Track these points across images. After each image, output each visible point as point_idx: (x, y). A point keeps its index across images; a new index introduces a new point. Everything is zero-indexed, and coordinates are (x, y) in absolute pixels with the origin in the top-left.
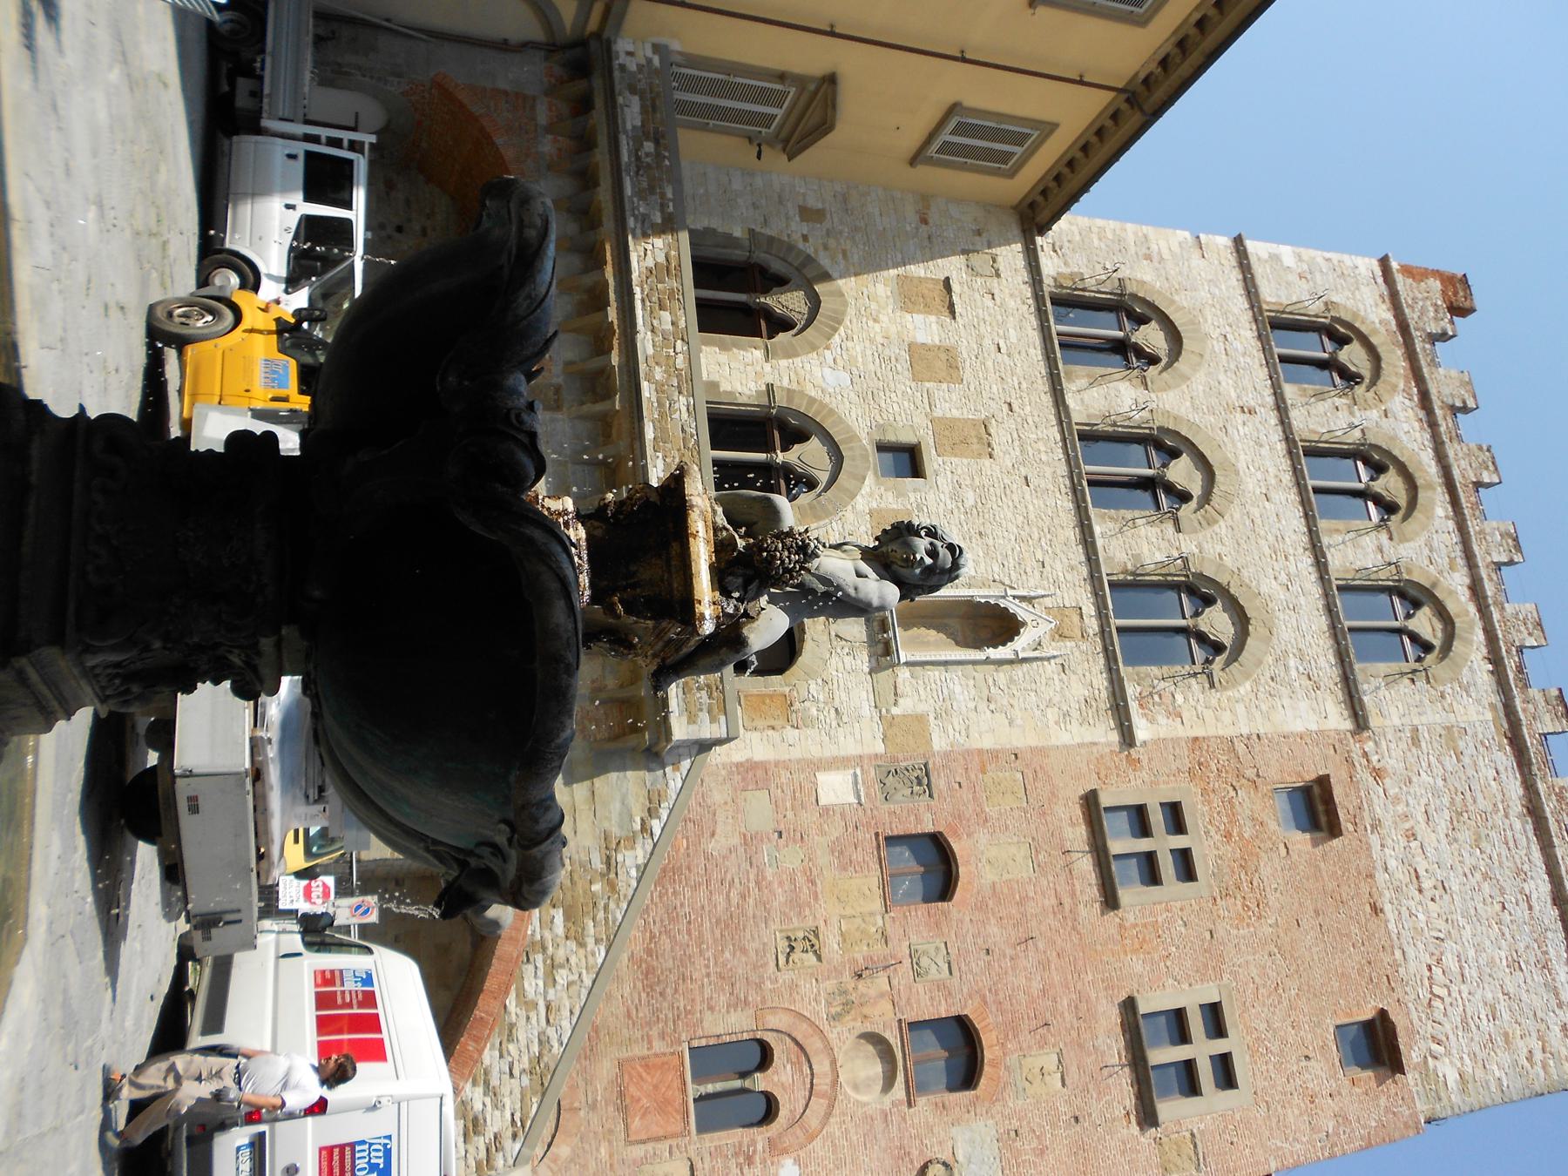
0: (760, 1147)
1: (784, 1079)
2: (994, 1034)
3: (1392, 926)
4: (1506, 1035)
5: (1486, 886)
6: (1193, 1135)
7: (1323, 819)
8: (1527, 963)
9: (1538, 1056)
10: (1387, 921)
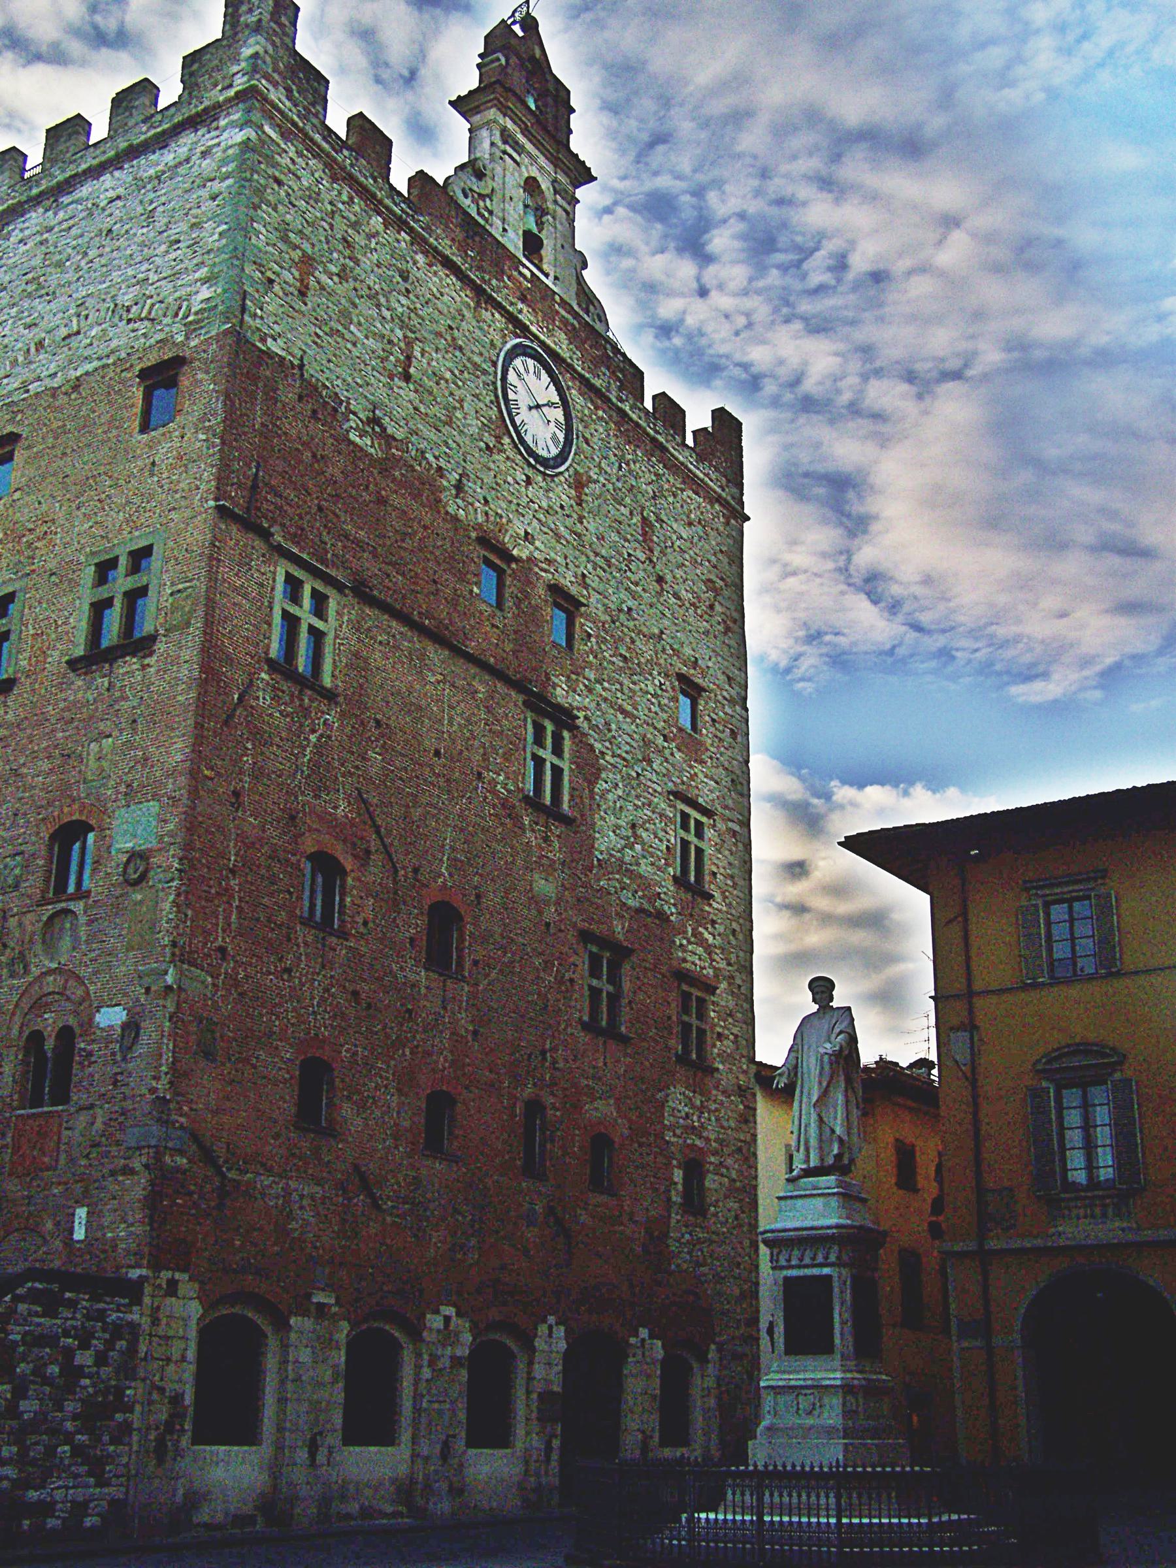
0: (82, 1045)
1: (51, 1021)
2: (66, 810)
3: (89, 367)
4: (193, 226)
5: (92, 253)
6: (172, 594)
7: (8, 449)
8: (152, 202)
9: (216, 186)
10: (87, 374)
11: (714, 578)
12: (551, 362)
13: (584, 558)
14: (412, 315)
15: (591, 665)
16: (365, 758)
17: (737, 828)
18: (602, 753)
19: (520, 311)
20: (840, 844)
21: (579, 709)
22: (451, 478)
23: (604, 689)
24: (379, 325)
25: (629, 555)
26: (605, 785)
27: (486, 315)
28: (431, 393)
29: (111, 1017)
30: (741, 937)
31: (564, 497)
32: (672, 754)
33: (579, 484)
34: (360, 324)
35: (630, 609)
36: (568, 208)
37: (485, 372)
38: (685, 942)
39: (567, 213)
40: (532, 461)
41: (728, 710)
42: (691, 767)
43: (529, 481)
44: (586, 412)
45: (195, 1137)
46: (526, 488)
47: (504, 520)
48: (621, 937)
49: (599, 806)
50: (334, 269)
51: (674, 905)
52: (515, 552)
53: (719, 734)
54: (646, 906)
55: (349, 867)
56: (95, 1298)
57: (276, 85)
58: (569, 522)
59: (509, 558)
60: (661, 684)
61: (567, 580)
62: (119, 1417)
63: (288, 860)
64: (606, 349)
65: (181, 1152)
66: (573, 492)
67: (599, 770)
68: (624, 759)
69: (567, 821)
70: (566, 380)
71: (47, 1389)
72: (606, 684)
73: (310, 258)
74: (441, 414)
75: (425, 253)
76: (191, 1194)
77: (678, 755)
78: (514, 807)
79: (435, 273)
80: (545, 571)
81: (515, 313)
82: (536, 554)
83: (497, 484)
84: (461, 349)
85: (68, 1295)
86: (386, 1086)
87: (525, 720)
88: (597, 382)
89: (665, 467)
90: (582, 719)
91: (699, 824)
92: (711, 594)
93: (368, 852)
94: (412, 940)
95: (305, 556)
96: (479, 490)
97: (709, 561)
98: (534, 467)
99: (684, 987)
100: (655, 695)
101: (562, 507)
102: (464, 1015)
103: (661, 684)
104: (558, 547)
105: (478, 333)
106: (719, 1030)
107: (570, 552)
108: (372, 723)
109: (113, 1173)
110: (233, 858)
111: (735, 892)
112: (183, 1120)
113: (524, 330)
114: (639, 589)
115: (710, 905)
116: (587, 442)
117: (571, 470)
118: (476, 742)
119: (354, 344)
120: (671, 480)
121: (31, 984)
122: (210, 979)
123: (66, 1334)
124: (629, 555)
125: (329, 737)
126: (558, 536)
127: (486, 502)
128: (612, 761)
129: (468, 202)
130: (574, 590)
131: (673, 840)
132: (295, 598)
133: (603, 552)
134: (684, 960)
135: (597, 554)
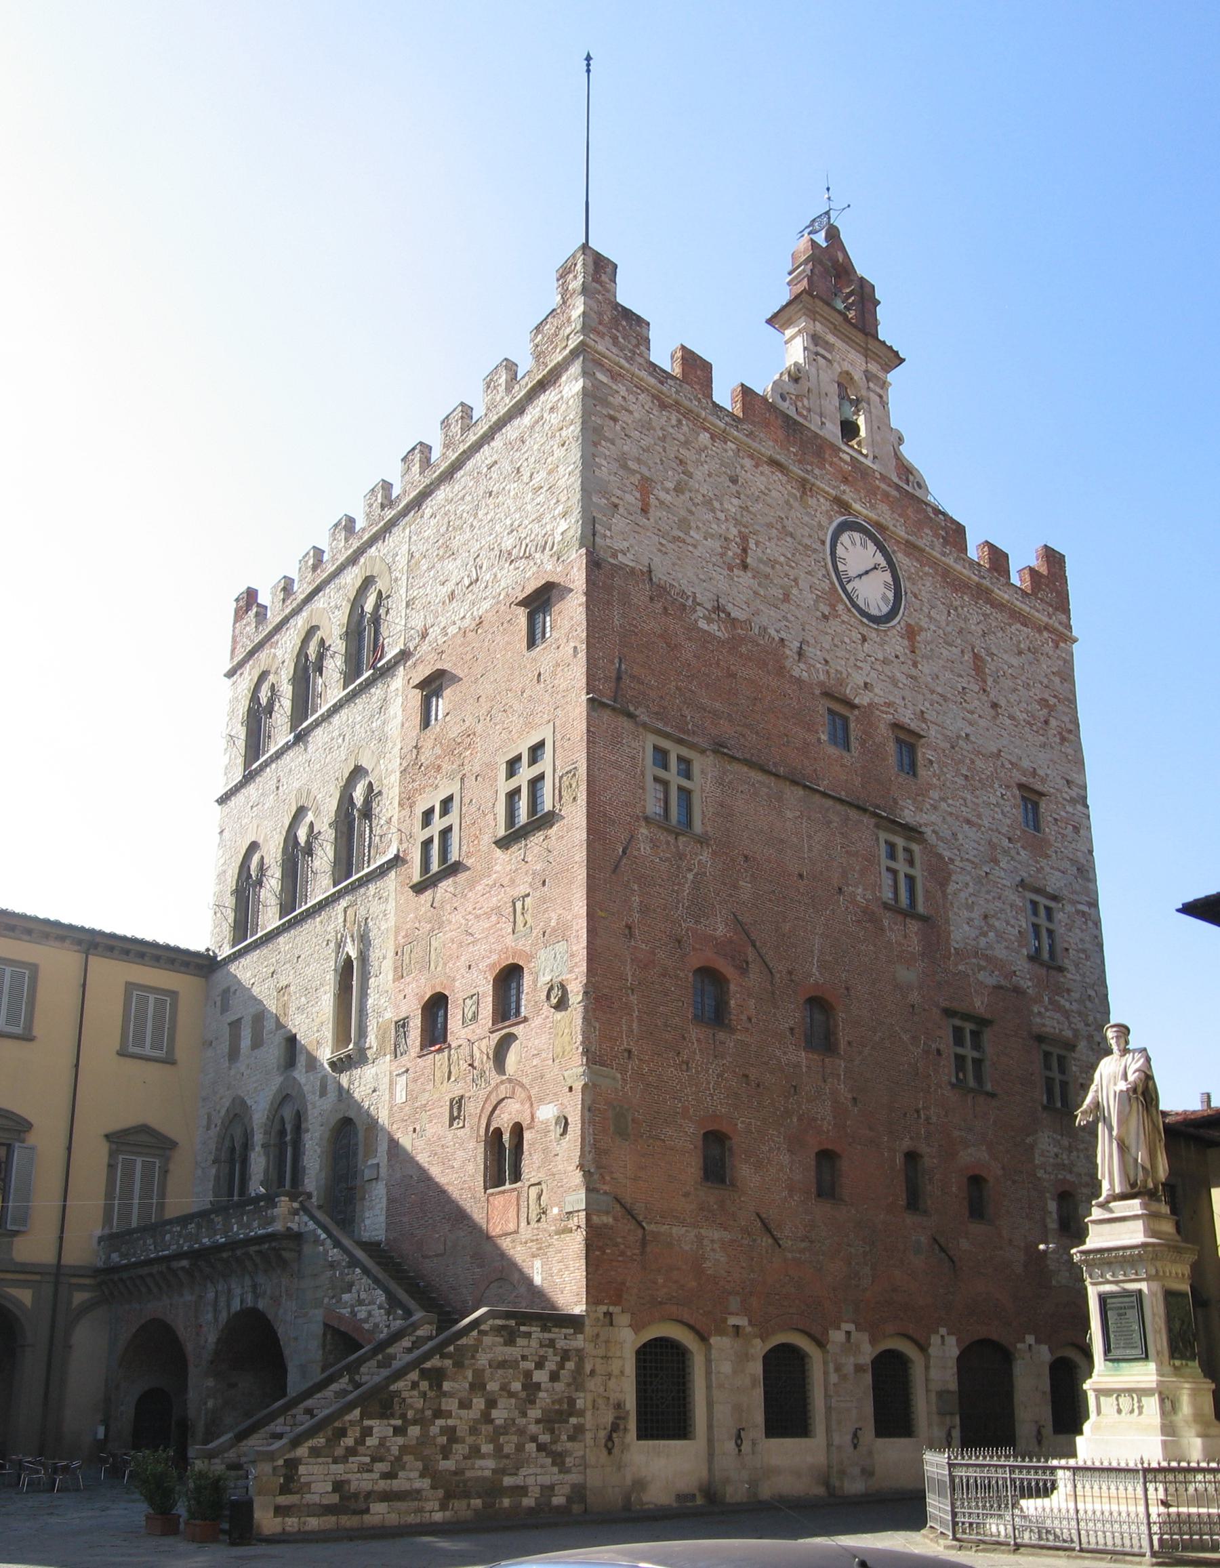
12: (876, 535)
13: (921, 697)
16: (735, 887)
20: (1178, 910)
21: (926, 825)
29: (547, 1113)
31: (898, 647)
33: (911, 633)
40: (865, 620)
43: (864, 639)
45: (618, 1200)
47: (844, 675)
52: (856, 701)
55: (729, 977)
56: (545, 1329)
58: (905, 668)
59: (853, 706)
61: (907, 717)
62: (573, 1420)
63: (677, 976)
64: (925, 511)
65: (607, 1213)
66: (906, 642)
69: (924, 919)
71: (513, 1401)
76: (616, 1245)
78: (873, 913)
83: (836, 646)
85: (522, 1328)
87: (877, 839)
88: (920, 543)
90: (929, 833)
93: (747, 963)
94: (792, 1029)
96: (819, 653)
101: (897, 657)
107: (907, 693)
108: (741, 859)
109: (558, 1233)
112: (606, 1188)
116: (916, 596)
117: (902, 623)
118: (835, 864)
121: (491, 1093)
122: (619, 1076)
123: (524, 1358)
127: (827, 662)
130: (913, 726)
132: (665, 767)
135: (933, 692)
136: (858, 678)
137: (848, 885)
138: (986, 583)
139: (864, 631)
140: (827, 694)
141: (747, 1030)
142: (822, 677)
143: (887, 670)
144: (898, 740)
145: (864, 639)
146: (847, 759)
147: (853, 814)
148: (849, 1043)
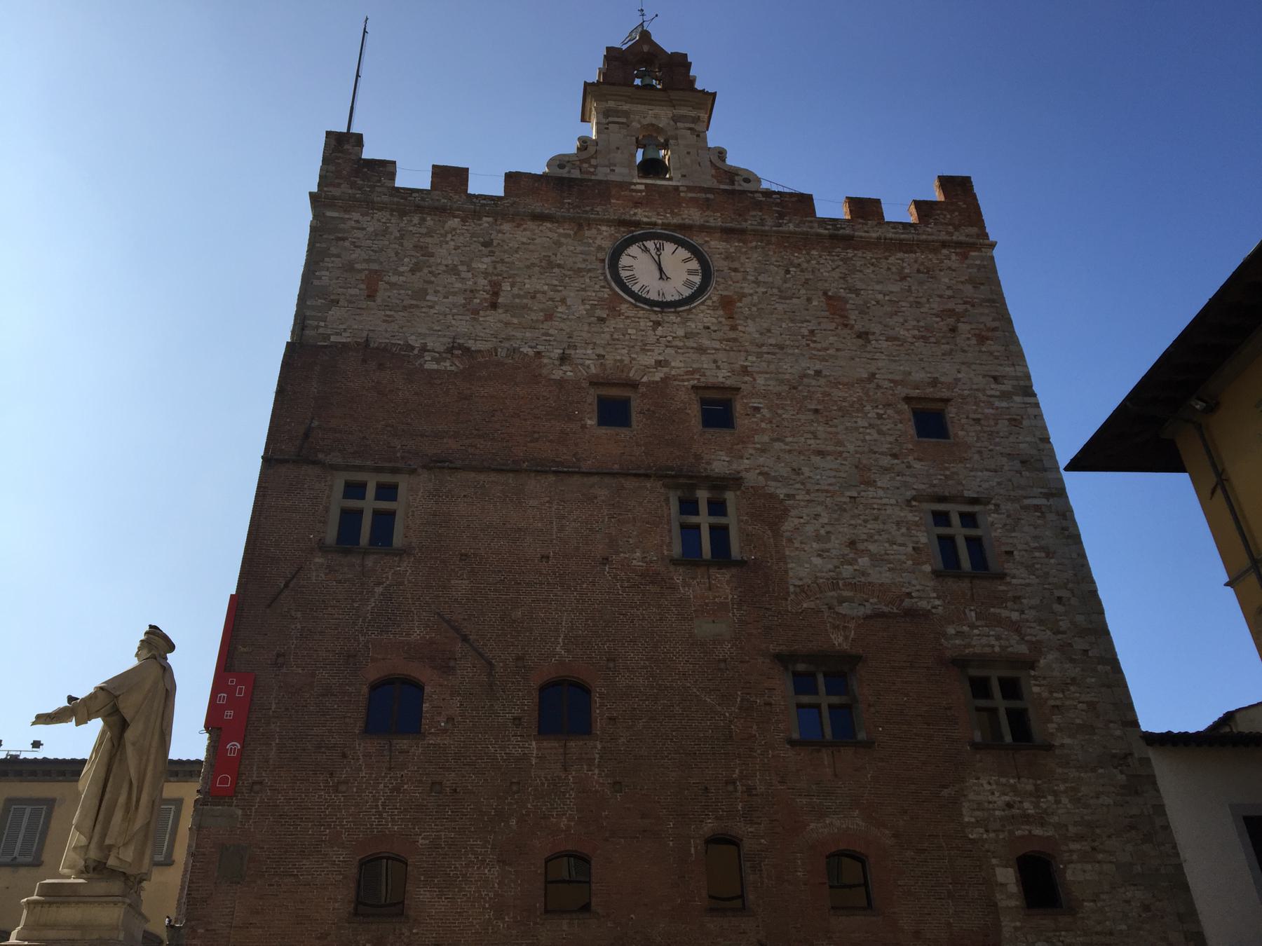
11: (950, 305)
12: (680, 235)
14: (499, 266)
15: (764, 431)
17: (1042, 501)
18: (790, 496)
19: (635, 214)
21: (747, 470)
22: (552, 355)
23: (786, 444)
24: (458, 285)
25: (812, 332)
26: (796, 521)
27: (594, 231)
28: (525, 307)
30: (1074, 601)
32: (909, 467)
33: (727, 304)
34: (436, 292)
35: (818, 373)
36: (692, 126)
37: (589, 271)
38: (965, 628)
39: (690, 129)
41: (1004, 404)
42: (947, 469)
44: (732, 250)
46: (654, 330)
48: (845, 646)
49: (790, 540)
50: (401, 269)
51: (938, 598)
53: (986, 429)
54: (886, 609)
57: (339, 185)
58: (720, 334)
59: (634, 385)
60: (880, 416)
61: (721, 376)
66: (721, 312)
67: (786, 511)
68: (827, 491)
69: (742, 563)
70: (697, 240)
72: (789, 439)
73: (376, 271)
74: (541, 316)
75: (513, 220)
77: (917, 465)
79: (525, 230)
80: (688, 380)
81: (627, 217)
82: (673, 373)
84: (559, 266)
86: (483, 861)
87: (667, 500)
88: (744, 225)
89: (855, 249)
91: (963, 515)
92: (951, 321)
94: (517, 721)
95: (369, 463)
96: (589, 352)
97: (940, 296)
98: (661, 312)
99: (974, 672)
100: (871, 426)
102: (596, 771)
103: (880, 416)
104: (704, 358)
105: (579, 249)
106: (1052, 703)
107: (721, 356)
110: (274, 706)
111: (1052, 561)
113: (637, 224)
114: (831, 352)
115: (1010, 583)
116: (735, 270)
117: (715, 299)
119: (431, 307)
120: (869, 255)
122: (240, 812)
124: (812, 332)
125: (402, 583)
126: (701, 350)
127: (598, 356)
128: (808, 497)
129: (567, 169)
130: (728, 383)
131: (924, 540)
133: (772, 341)
134: (969, 646)
136: (648, 360)
137: (617, 553)
138: (848, 231)
139: (659, 318)
140: (592, 384)
141: (445, 731)
142: (593, 370)
143: (691, 343)
144: (703, 402)
145: (657, 324)
146: (623, 432)
147: (630, 484)
148: (612, 719)
